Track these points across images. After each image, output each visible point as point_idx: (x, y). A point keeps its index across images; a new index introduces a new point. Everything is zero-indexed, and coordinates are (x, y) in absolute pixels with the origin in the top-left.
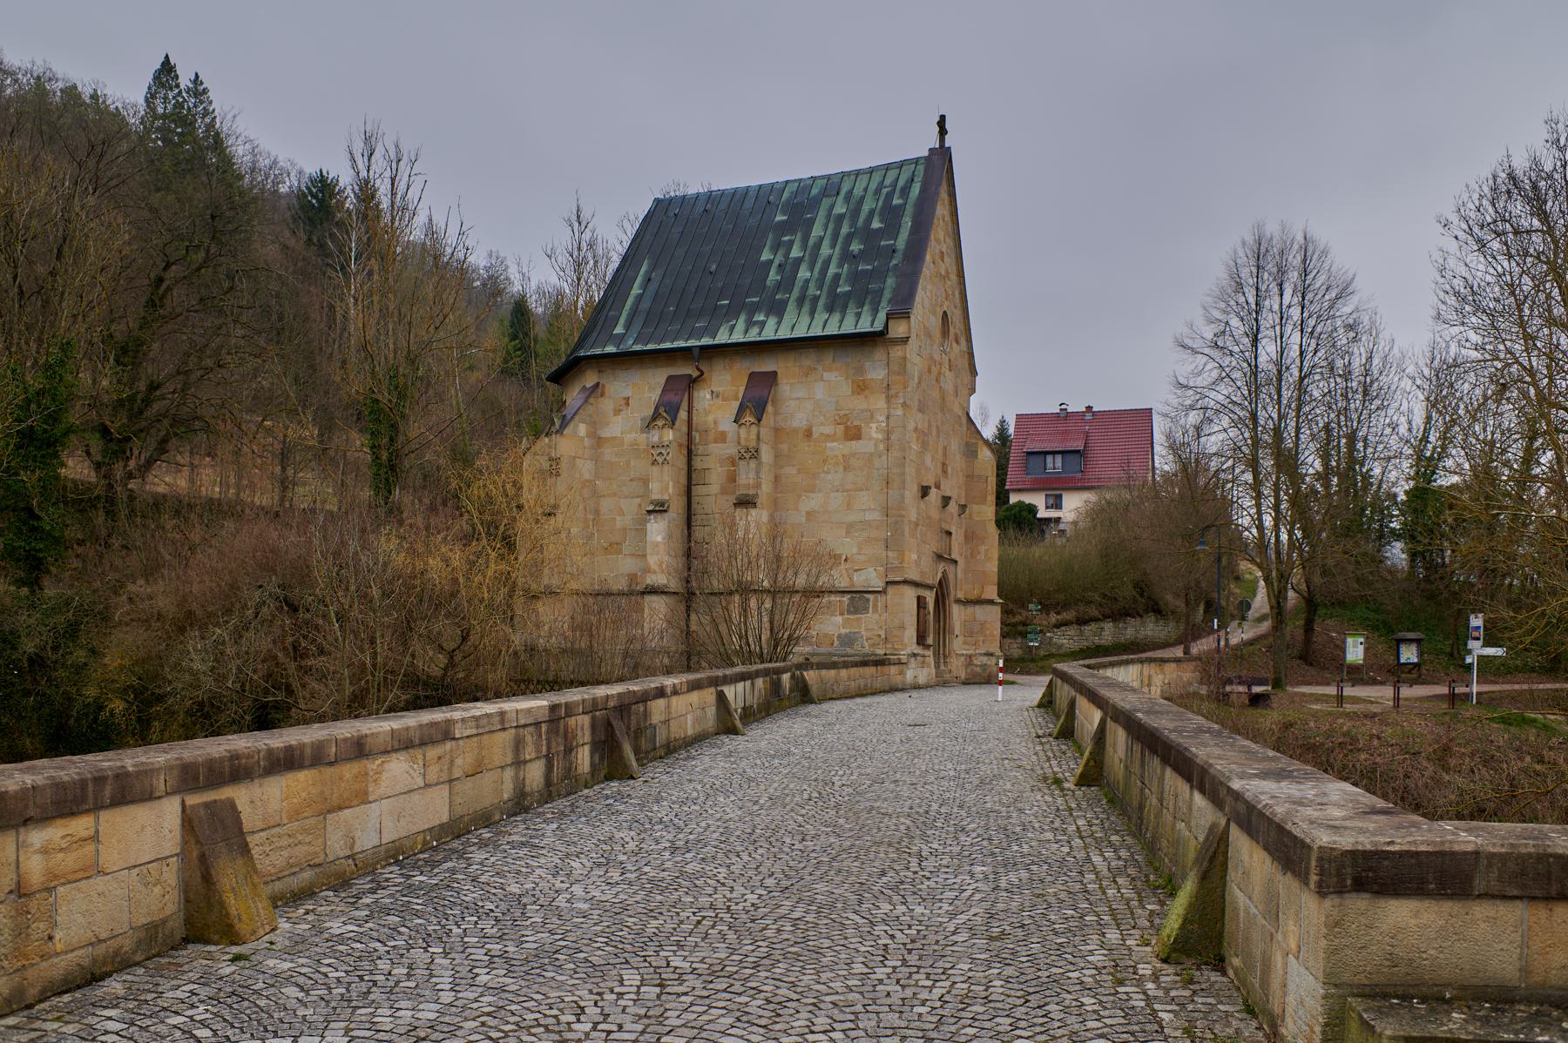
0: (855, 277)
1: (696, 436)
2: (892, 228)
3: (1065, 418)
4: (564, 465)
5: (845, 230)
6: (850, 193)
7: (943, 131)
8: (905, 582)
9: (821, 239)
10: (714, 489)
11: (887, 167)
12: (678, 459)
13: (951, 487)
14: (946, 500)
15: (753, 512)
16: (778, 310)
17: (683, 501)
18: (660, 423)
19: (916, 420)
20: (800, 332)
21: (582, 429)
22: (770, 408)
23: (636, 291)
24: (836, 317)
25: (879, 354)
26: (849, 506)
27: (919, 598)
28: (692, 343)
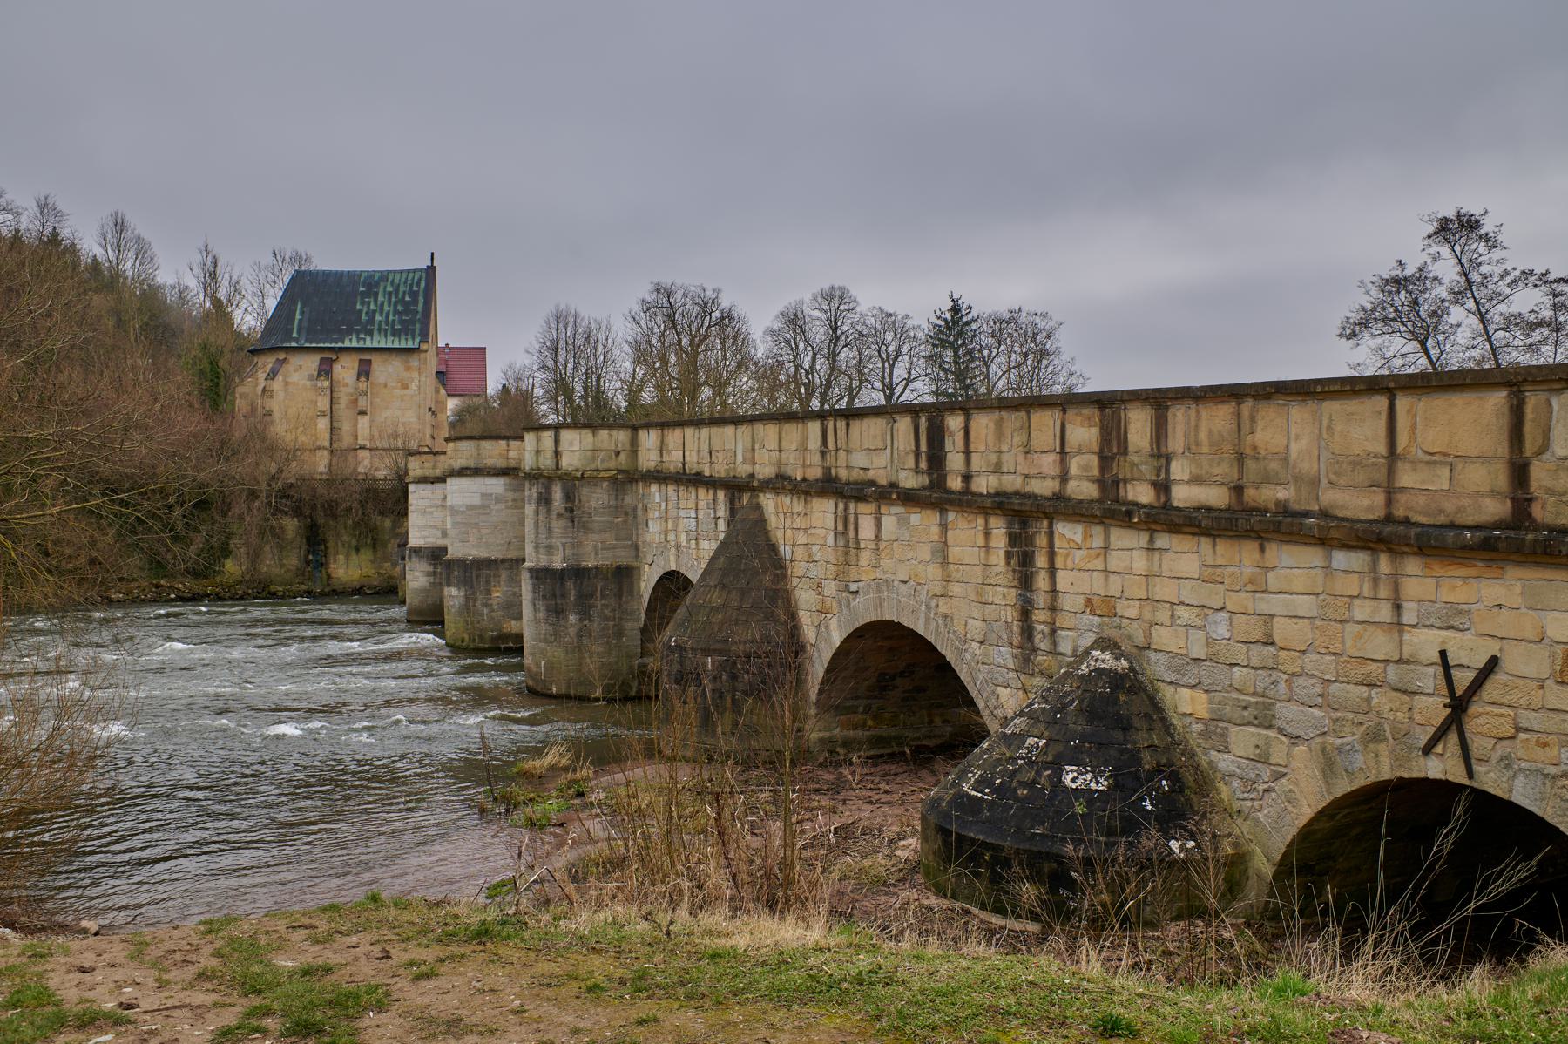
0: (402, 322)
1: (334, 384)
2: (415, 302)
5: (393, 299)
6: (392, 282)
10: (343, 406)
11: (409, 271)
12: (328, 392)
16: (370, 333)
23: (298, 317)
25: (416, 356)
28: (333, 345)
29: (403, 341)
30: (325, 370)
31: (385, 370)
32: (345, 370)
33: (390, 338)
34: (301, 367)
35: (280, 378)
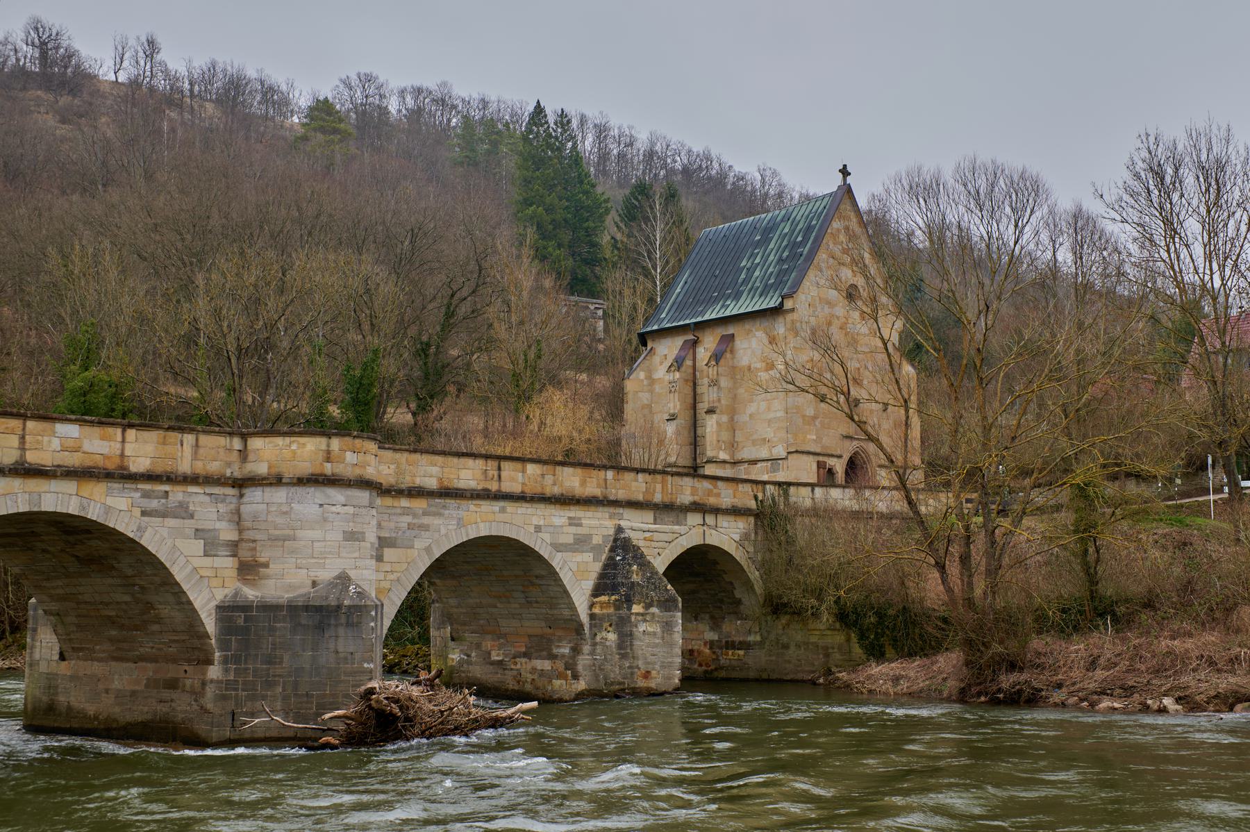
7: (845, 172)
8: (797, 452)
15: (714, 416)
17: (689, 413)
18: (673, 369)
21: (642, 375)
22: (728, 355)
23: (678, 290)
25: (781, 319)
26: (769, 409)
27: (818, 462)
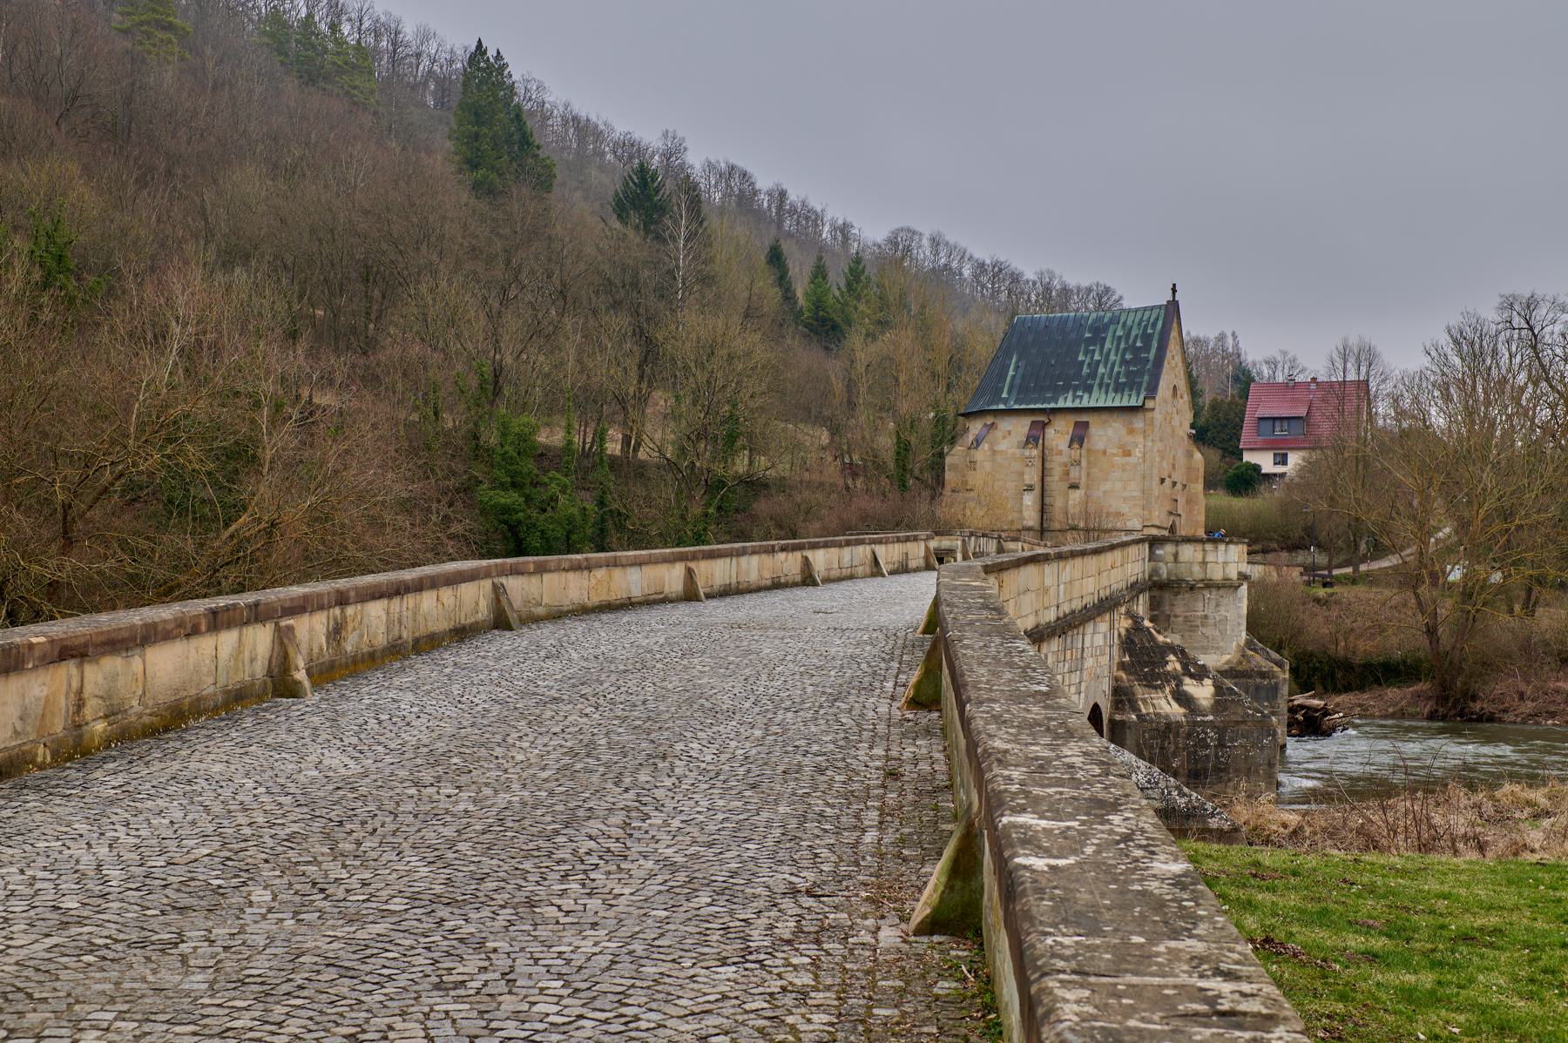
0: (1128, 374)
2: (1147, 348)
3: (1293, 387)
4: (978, 465)
5: (1122, 346)
7: (1174, 290)
9: (1110, 350)
10: (1056, 478)
11: (1145, 309)
12: (1038, 463)
13: (1177, 476)
14: (1174, 484)
16: (1089, 389)
19: (1159, 446)
20: (1100, 404)
23: (1011, 373)
24: (1119, 396)
25: (1140, 415)
28: (1045, 406)
29: (1126, 398)
30: (1035, 437)
31: (1104, 434)
32: (1058, 434)
33: (1111, 395)
34: (1009, 432)
35: (985, 446)
